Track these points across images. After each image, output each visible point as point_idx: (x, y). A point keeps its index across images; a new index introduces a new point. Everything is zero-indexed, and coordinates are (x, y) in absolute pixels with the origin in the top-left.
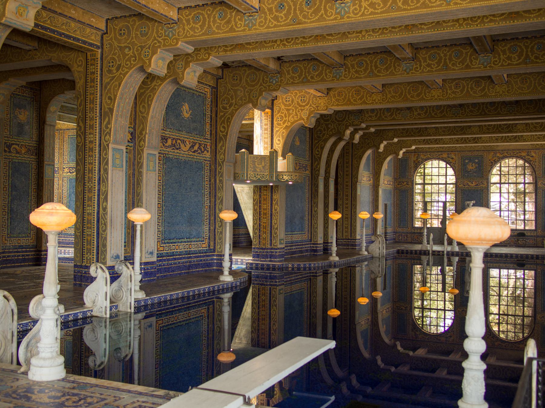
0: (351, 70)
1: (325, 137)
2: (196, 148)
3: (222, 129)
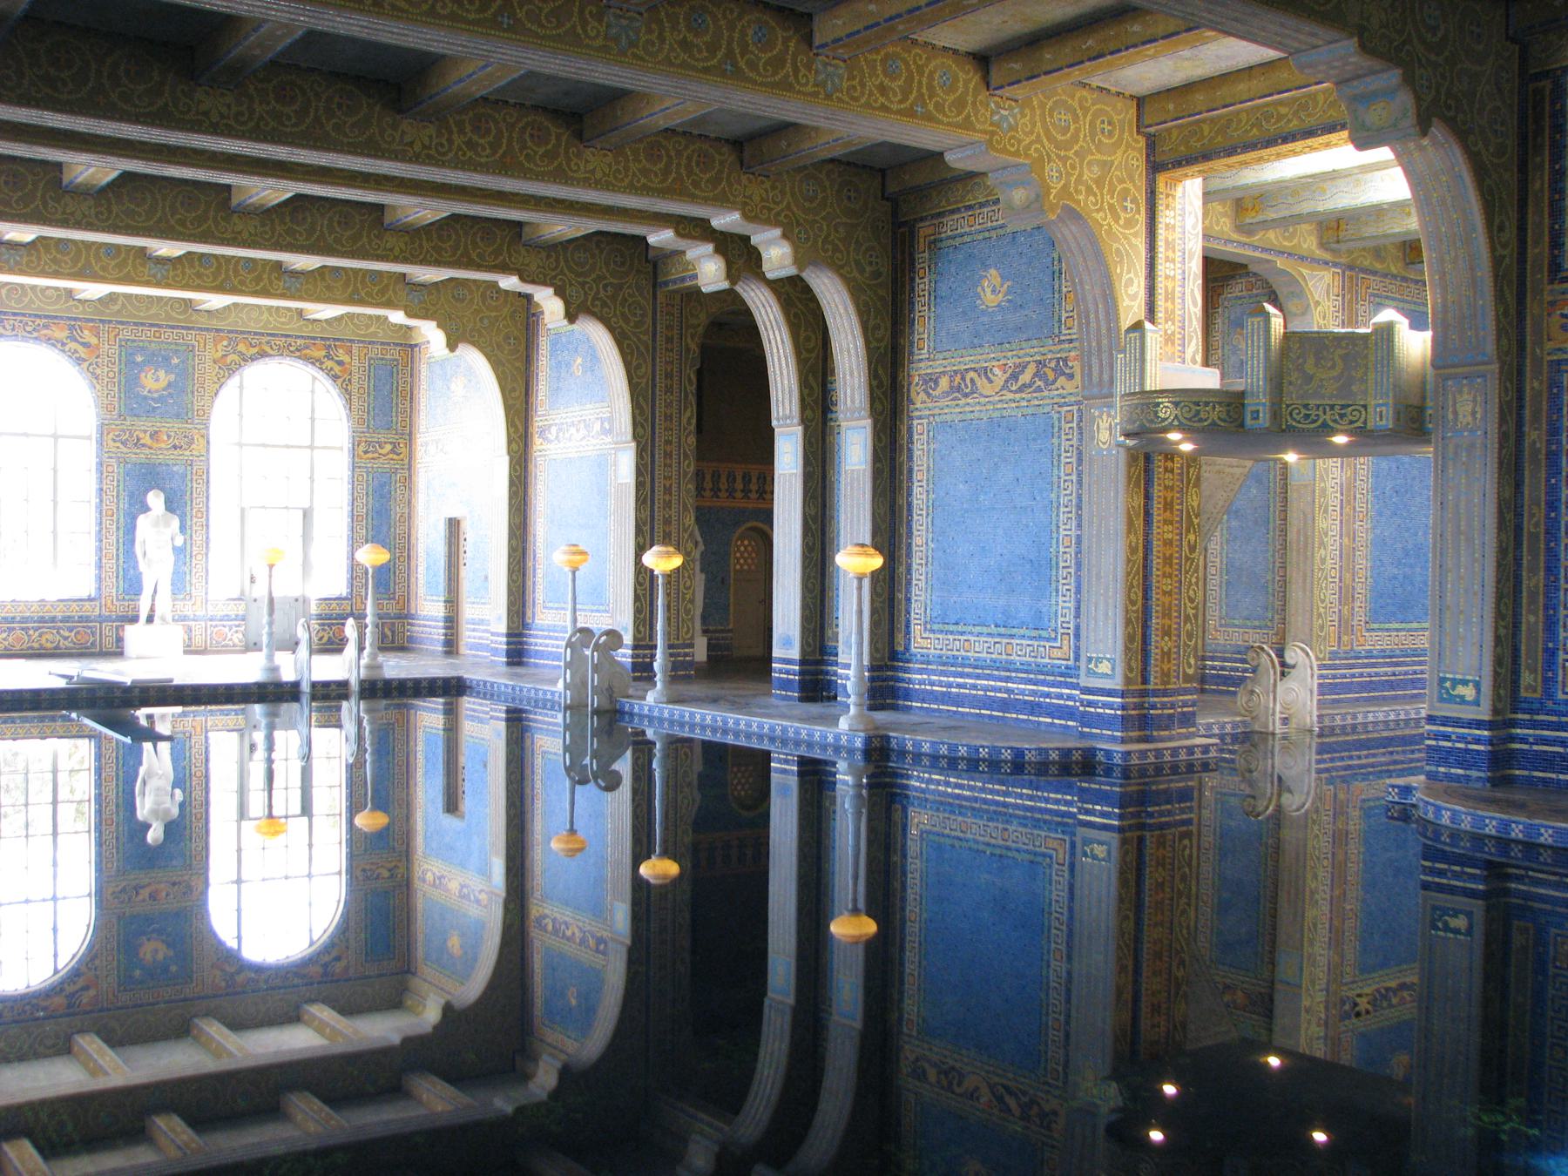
2: (1025, 378)
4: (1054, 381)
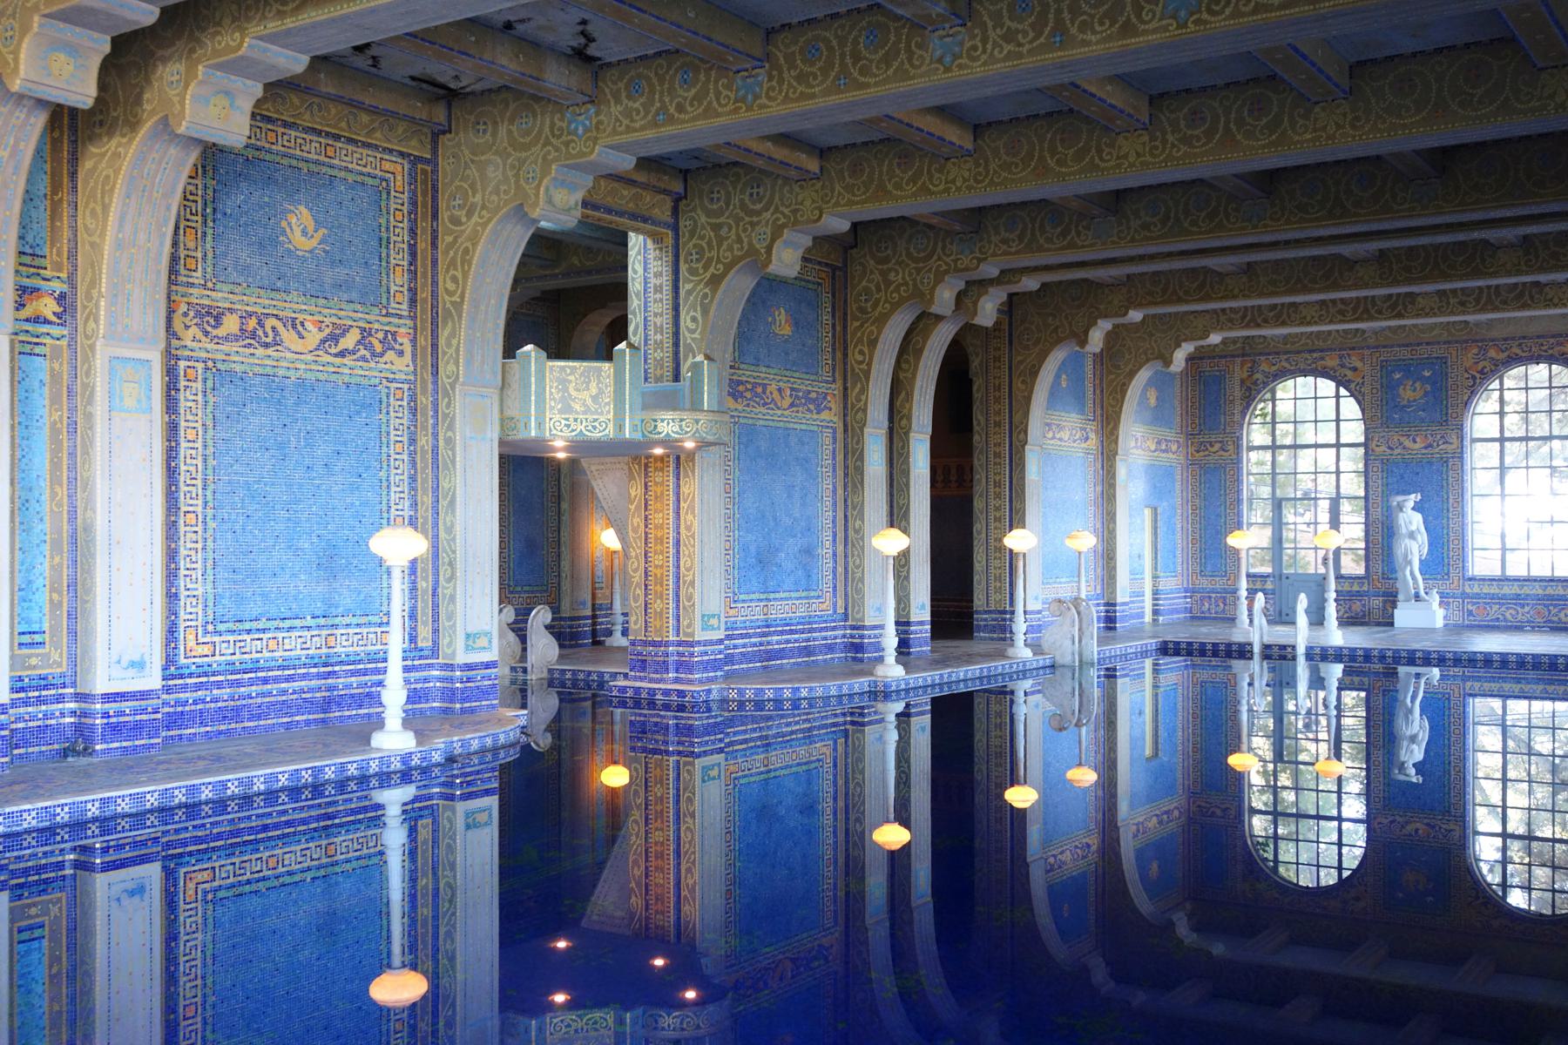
0: (786, 75)
1: (879, 309)
2: (349, 341)
3: (451, 286)
4: (381, 355)
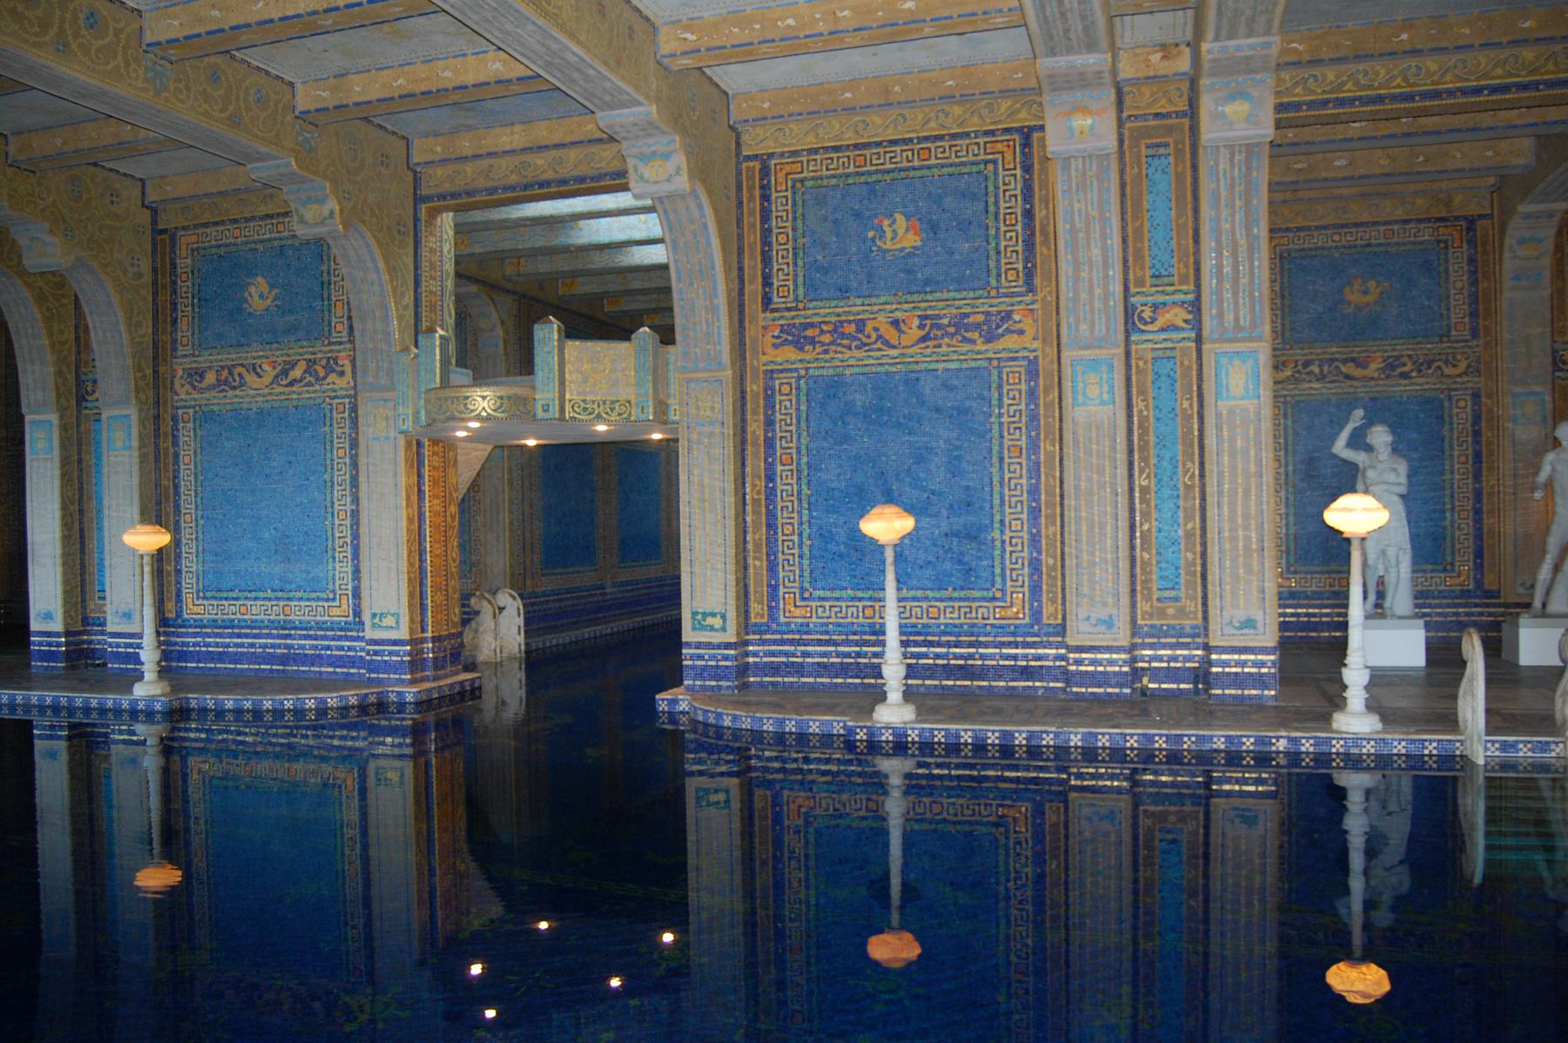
2: (297, 373)
4: (325, 378)
